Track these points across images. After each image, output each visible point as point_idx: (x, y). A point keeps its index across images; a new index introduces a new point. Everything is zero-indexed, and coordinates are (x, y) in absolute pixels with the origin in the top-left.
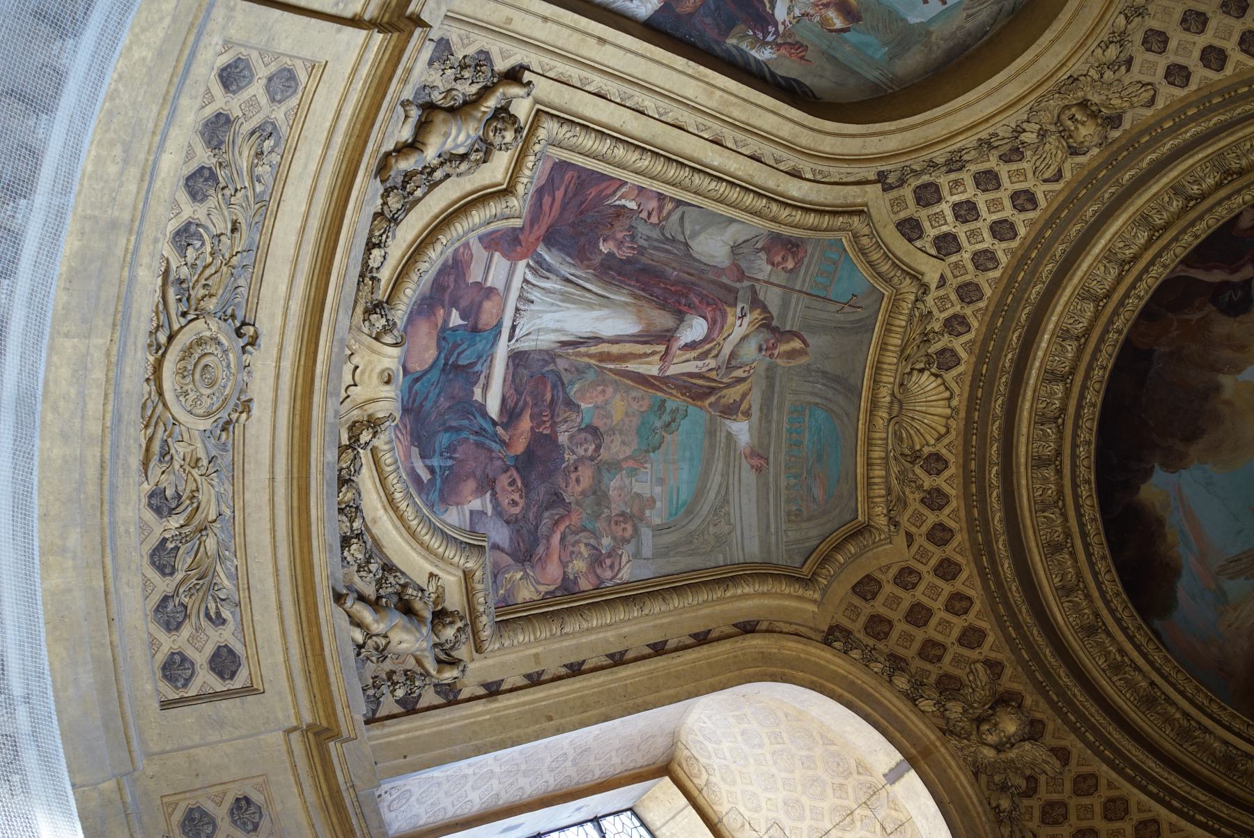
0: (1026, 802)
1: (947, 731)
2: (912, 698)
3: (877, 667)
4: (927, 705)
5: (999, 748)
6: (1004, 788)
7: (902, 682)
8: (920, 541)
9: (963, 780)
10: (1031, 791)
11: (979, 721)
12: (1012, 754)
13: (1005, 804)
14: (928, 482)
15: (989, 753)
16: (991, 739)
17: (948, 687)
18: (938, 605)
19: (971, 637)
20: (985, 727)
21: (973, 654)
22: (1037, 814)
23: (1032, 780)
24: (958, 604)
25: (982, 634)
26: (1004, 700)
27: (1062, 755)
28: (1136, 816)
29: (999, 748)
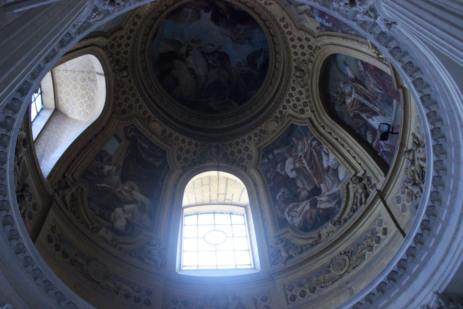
0: (120, 89)
1: (114, 71)
2: (111, 62)
3: (108, 55)
4: (113, 65)
5: (121, 77)
6: (118, 85)
7: (111, 59)
8: (128, 31)
9: (112, 82)
10: (122, 87)
11: (120, 71)
12: (122, 79)
13: (117, 89)
14: (136, 20)
15: (119, 78)
16: (121, 75)
17: (118, 62)
18: (123, 44)
19: (126, 52)
20: (120, 73)
21: (124, 56)
22: (121, 92)
23: (123, 85)
24: (127, 45)
25: (128, 52)
26: (126, 68)
27: (130, 81)
28: (136, 98)
29: (121, 77)
